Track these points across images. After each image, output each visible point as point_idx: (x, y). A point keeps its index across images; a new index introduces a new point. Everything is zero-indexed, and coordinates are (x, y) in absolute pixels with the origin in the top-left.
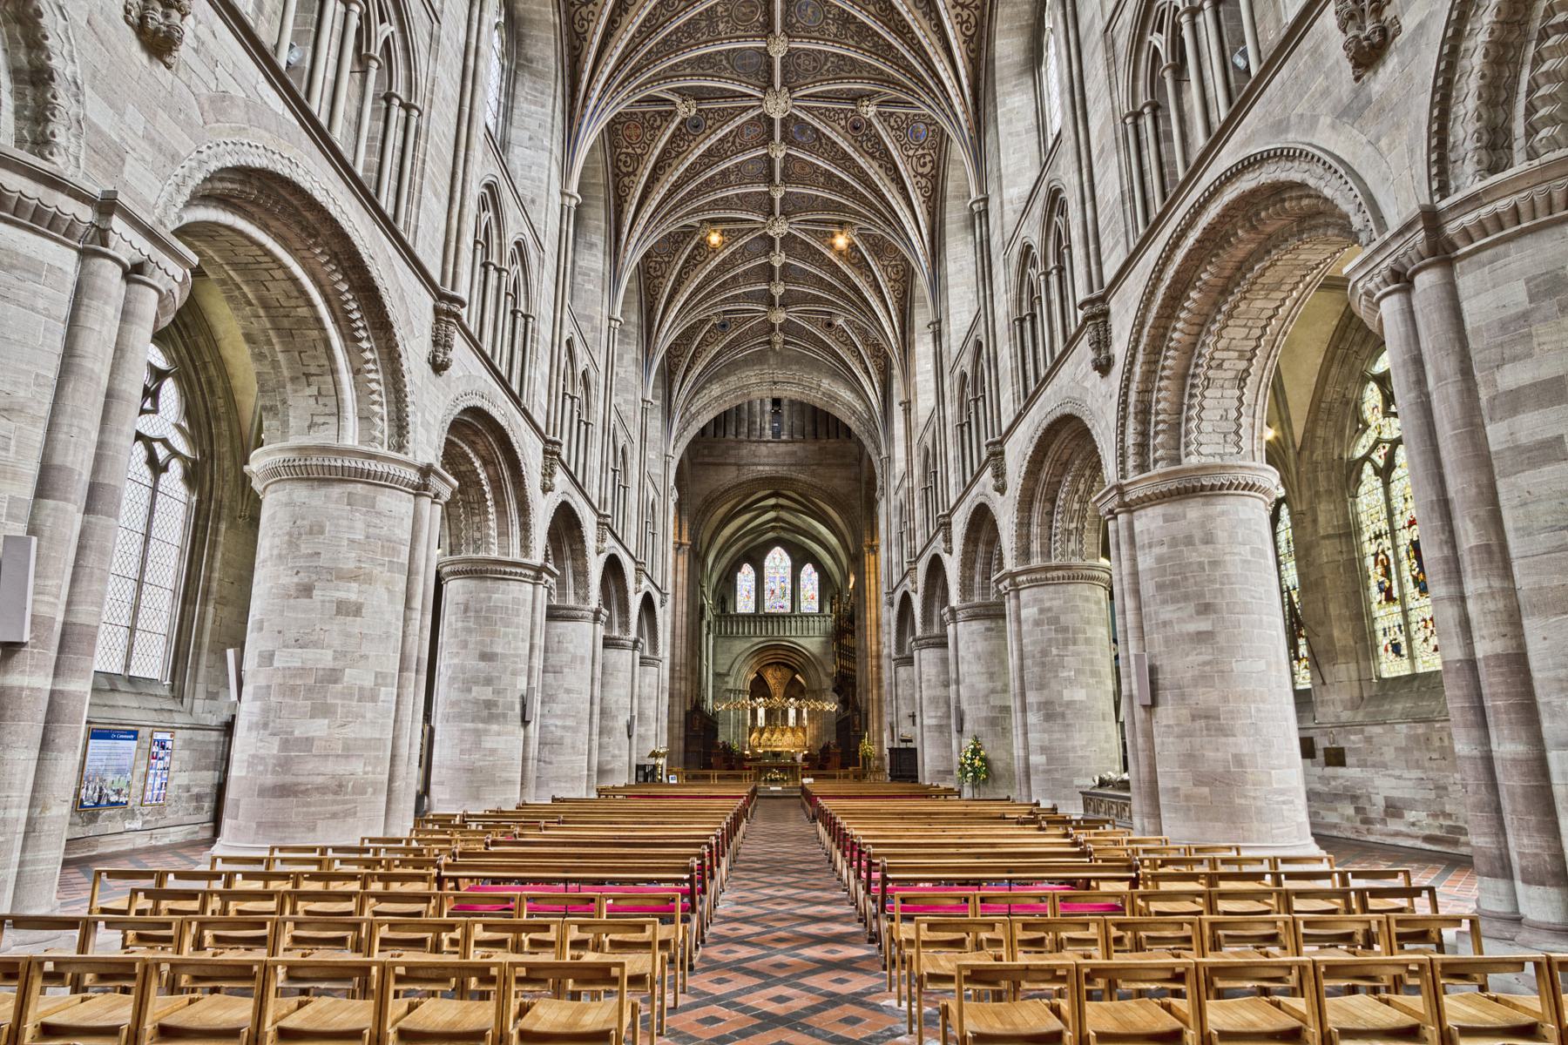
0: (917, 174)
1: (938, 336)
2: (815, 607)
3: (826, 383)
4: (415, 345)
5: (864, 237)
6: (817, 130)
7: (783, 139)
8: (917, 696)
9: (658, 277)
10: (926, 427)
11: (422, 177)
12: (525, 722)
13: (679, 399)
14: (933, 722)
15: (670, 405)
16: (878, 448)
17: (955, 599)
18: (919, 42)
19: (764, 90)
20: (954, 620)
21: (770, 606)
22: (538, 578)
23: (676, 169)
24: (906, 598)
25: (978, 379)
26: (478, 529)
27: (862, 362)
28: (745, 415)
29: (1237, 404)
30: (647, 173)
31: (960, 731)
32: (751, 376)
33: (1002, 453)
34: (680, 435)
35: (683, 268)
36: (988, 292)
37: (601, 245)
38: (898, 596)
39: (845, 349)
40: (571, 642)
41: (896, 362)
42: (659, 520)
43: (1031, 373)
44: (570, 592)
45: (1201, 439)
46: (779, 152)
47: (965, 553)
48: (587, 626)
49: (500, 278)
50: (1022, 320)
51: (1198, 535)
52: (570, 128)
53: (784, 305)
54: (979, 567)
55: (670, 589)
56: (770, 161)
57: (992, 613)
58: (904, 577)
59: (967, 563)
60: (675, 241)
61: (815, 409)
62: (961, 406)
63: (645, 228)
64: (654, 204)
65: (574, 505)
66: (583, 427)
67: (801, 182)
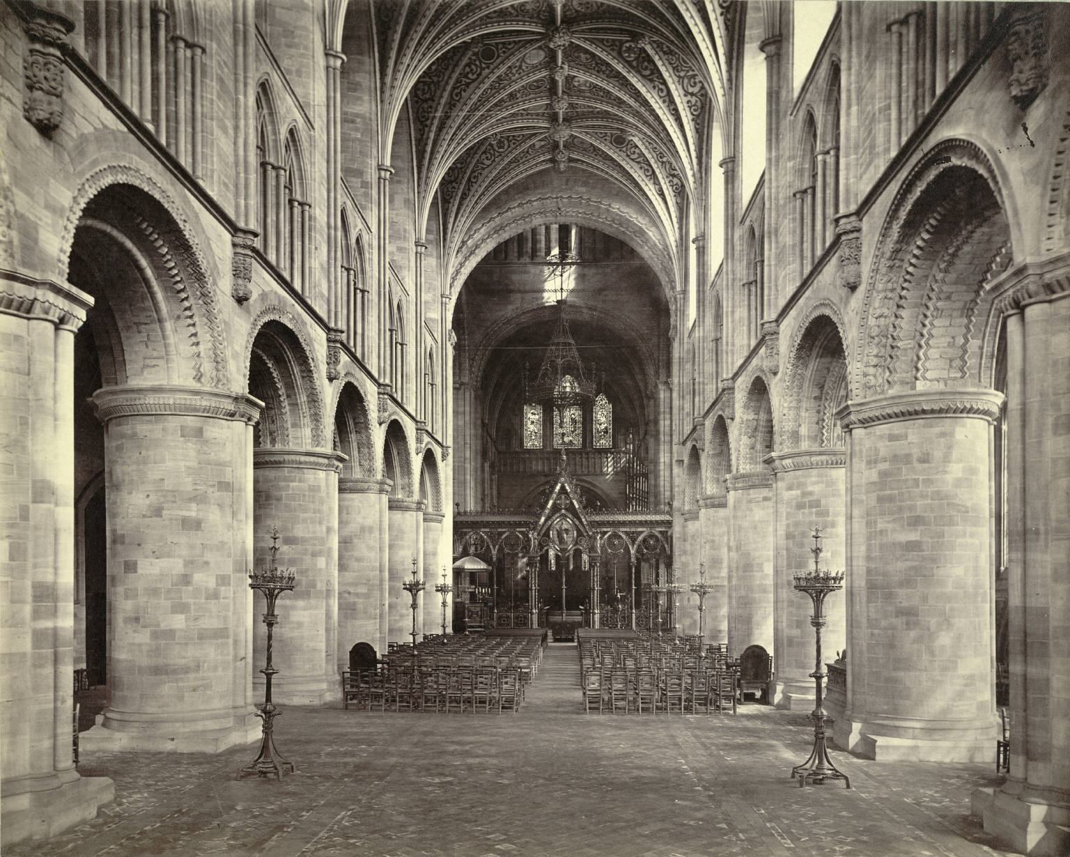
1: (731, 178)
9: (426, 101)
27: (656, 182)
29: (964, 331)
39: (636, 166)
42: (438, 369)
45: (927, 364)
48: (372, 497)
51: (916, 453)
55: (450, 442)
65: (355, 383)
66: (359, 295)
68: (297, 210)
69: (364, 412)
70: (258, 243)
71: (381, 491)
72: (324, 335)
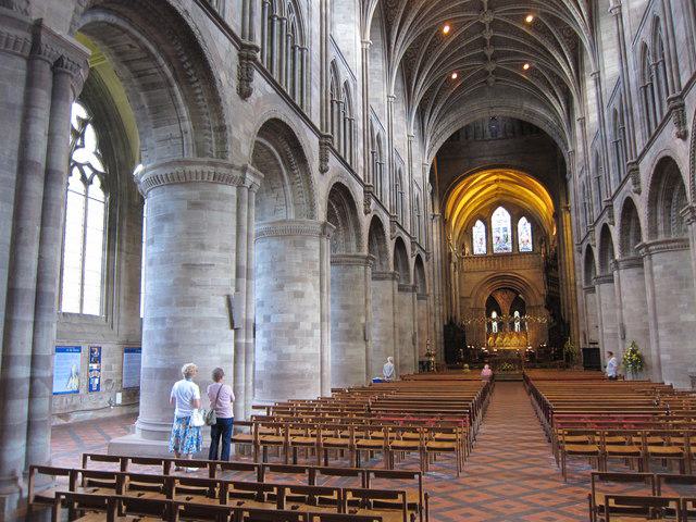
1: (598, 82)
2: (531, 248)
3: (526, 105)
4: (314, 165)
5: (545, 15)
13: (429, 126)
20: (617, 268)
24: (589, 250)
27: (551, 88)
28: (471, 133)
31: (624, 338)
32: (475, 105)
33: (637, 169)
34: (431, 150)
38: (584, 247)
41: (573, 90)
47: (622, 225)
49: (339, 106)
53: (494, 58)
54: (632, 234)
57: (637, 263)
58: (587, 236)
59: (624, 231)
60: (422, 37)
61: (521, 122)
69: (383, 233)
70: (329, 141)
71: (393, 279)
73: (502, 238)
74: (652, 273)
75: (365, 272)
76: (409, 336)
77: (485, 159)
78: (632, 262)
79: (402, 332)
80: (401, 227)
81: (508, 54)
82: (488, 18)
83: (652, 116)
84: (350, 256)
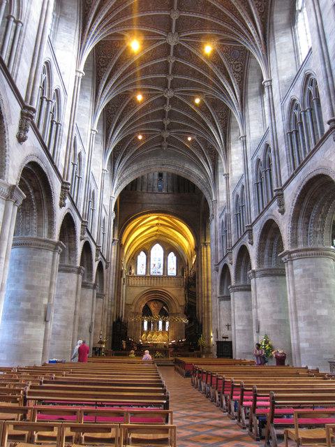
0: (234, 72)
3: (187, 166)
6: (190, 51)
7: (174, 55)
8: (232, 315)
10: (238, 185)
11: (21, 53)
12: (46, 321)
13: (119, 169)
14: (241, 328)
15: (113, 173)
16: (211, 196)
17: (254, 267)
18: (240, 14)
19: (167, 33)
21: (153, 272)
22: (56, 249)
23: (125, 66)
24: (226, 267)
25: (268, 162)
26: (29, 223)
30: (112, 67)
32: (152, 161)
33: (282, 194)
34: (118, 188)
35: (124, 110)
36: (273, 121)
37: (89, 97)
40: (67, 283)
43: (296, 158)
44: (67, 258)
46: (172, 60)
49: (48, 104)
50: (291, 133)
52: (81, 44)
53: (168, 129)
56: (167, 63)
59: (261, 249)
62: (257, 175)
63: (110, 91)
64: (114, 80)
65: (72, 215)
67: (181, 73)
68: (55, 126)
69: (74, 232)
71: (79, 273)
72: (60, 185)
73: (157, 266)
74: (293, 275)
75: (54, 257)
76: (87, 325)
77: (153, 205)
78: (266, 272)
79: (81, 321)
80: (90, 234)
81: (179, 126)
82: (169, 94)
83: (296, 154)
84: (41, 240)
